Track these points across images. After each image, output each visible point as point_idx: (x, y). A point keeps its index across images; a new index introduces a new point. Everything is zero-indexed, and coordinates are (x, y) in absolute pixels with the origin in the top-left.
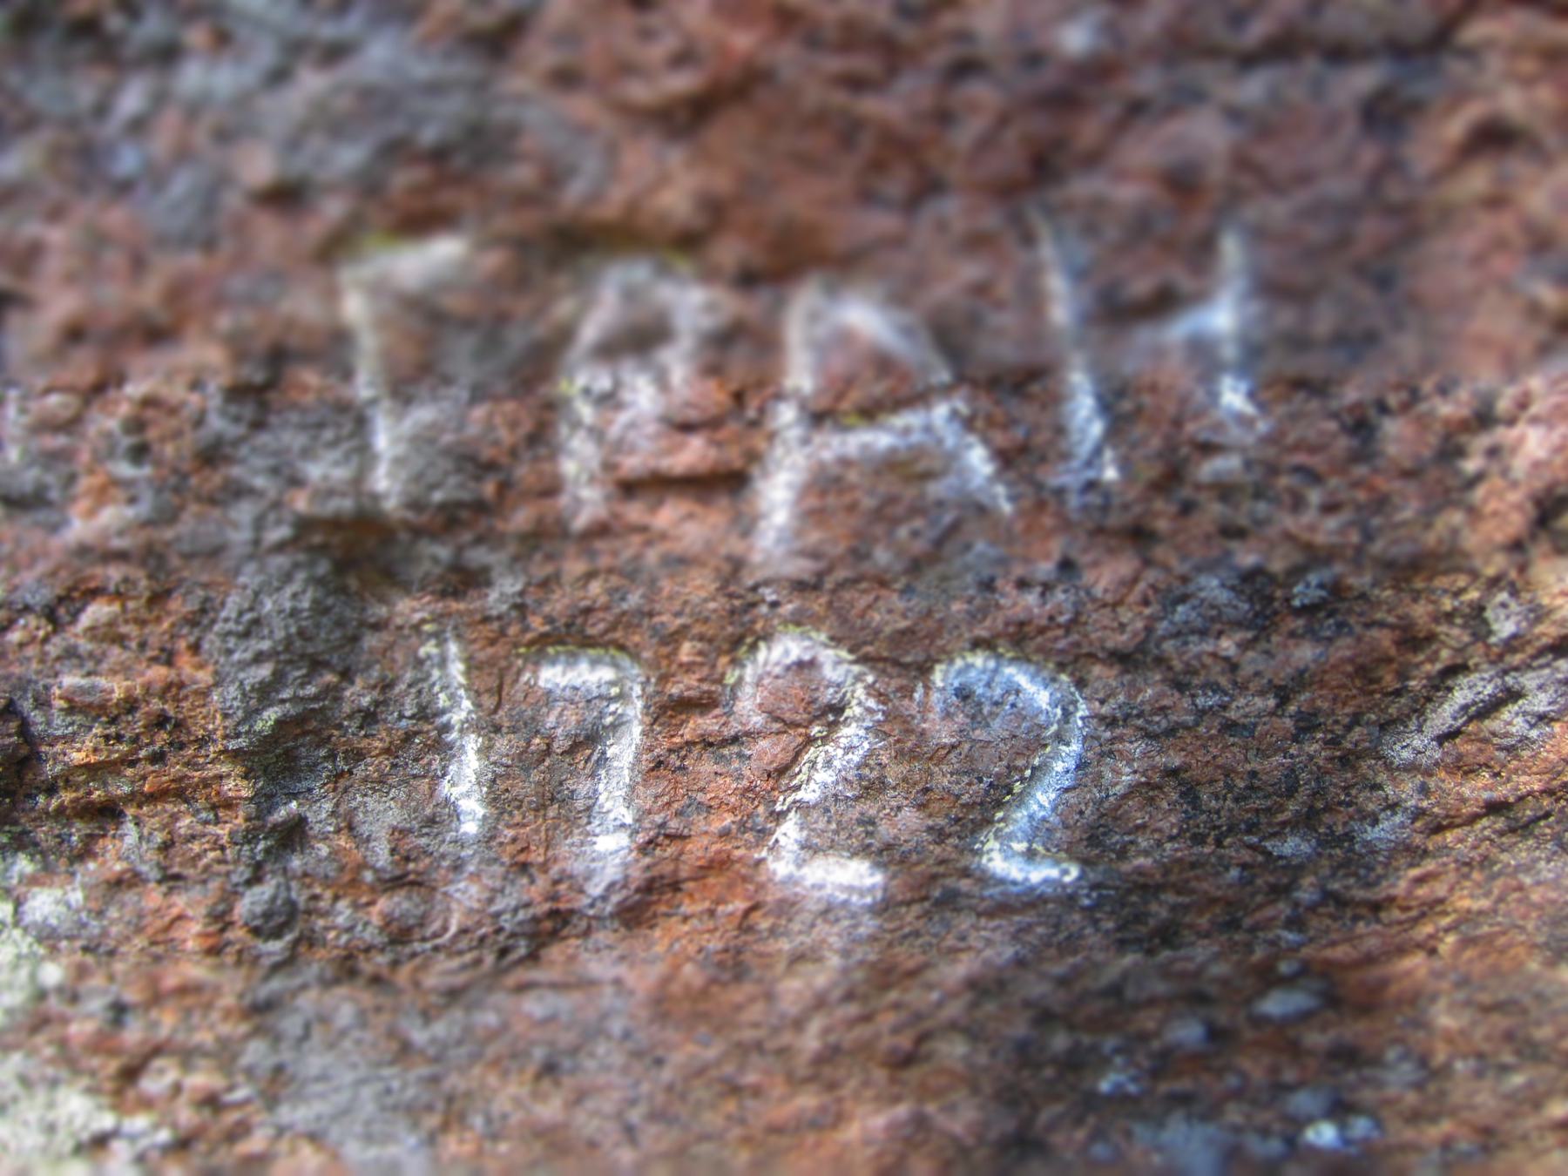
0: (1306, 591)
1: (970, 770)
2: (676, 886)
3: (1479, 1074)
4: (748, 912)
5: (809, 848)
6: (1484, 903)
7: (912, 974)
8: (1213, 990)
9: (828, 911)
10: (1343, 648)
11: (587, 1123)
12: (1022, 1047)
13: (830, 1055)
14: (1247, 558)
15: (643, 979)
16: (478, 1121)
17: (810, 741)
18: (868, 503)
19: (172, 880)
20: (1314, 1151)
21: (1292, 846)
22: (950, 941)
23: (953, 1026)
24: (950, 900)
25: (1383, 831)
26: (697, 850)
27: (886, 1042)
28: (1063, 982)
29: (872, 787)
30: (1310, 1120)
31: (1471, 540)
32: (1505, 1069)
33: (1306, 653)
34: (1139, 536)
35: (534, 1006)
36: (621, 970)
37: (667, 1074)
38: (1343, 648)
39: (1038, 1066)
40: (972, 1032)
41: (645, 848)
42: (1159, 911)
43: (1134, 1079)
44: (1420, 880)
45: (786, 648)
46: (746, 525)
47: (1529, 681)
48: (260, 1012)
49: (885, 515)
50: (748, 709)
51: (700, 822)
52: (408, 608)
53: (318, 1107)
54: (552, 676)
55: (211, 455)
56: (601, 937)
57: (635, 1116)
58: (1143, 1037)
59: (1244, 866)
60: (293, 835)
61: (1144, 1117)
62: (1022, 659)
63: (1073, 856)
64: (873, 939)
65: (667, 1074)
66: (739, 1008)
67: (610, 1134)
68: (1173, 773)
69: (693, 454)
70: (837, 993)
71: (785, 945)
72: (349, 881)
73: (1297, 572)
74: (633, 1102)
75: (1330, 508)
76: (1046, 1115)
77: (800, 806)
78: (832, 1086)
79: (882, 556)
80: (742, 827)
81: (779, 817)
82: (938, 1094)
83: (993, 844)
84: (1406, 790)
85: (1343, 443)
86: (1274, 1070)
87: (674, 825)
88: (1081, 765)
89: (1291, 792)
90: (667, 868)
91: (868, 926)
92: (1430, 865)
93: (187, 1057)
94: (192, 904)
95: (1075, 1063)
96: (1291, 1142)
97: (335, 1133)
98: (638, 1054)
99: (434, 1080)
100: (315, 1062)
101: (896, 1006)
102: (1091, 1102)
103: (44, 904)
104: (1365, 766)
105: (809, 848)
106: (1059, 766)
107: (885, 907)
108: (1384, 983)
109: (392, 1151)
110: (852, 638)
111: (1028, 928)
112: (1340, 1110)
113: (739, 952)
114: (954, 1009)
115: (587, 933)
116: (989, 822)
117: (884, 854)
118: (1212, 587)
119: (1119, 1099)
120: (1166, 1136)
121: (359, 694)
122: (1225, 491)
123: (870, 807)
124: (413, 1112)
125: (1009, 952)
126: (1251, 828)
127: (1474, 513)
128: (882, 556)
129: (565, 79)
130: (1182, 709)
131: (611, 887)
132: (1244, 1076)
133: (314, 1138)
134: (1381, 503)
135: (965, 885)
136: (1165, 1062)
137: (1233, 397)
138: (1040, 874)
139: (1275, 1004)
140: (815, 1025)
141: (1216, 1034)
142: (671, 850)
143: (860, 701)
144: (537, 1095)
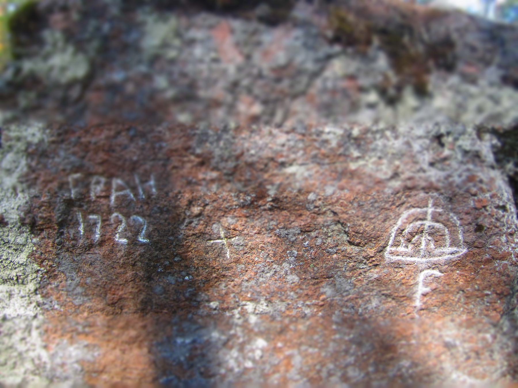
0: (165, 209)
1: (135, 228)
2: (105, 241)
3: (203, 270)
4: (113, 245)
5: (120, 238)
6: (196, 246)
7: (133, 253)
8: (168, 257)
9: (122, 245)
10: (170, 216)
11: (95, 271)
12: (147, 264)
13: (124, 264)
14: (158, 206)
15: (102, 253)
16: (82, 271)
17: (118, 225)
18: (121, 199)
19: (49, 238)
20: (186, 280)
21: (171, 238)
22: (137, 249)
23: (138, 260)
24: (136, 244)
25: (181, 237)
26: (107, 237)
27: (131, 262)
28: (150, 255)
29: (126, 230)
30: (185, 276)
31: (181, 205)
32: (206, 269)
33: (167, 216)
34: (147, 203)
35: (89, 256)
36: (99, 252)
37: (105, 265)
38: (170, 216)
39: (150, 267)
40: (142, 262)
41: (101, 236)
42: (159, 245)
43: (162, 269)
44: (187, 243)
45: (115, 215)
46: (110, 201)
47: (194, 220)
48: (58, 254)
49: (123, 200)
50: (112, 221)
51: (107, 234)
52: (75, 209)
53: (64, 268)
54: (91, 217)
55: (56, 193)
56: (97, 248)
57: (101, 271)
58: (162, 264)
59: (167, 240)
60: (62, 233)
61: (166, 275)
62: (139, 216)
63: (148, 239)
64: (127, 248)
65: (105, 265)
66: (113, 257)
67: (98, 273)
68: (156, 229)
69: (103, 194)
70: (124, 255)
71: (118, 249)
72: (68, 239)
73: (164, 207)
74: (101, 269)
75: (165, 201)
76: (153, 274)
77: (119, 232)
78: (125, 268)
79: (123, 205)
80: (112, 234)
81: (116, 234)
82: (139, 270)
83: (139, 237)
84: (183, 232)
85: (165, 195)
86: (179, 269)
87: (104, 234)
88: (147, 228)
89: (169, 231)
90: (104, 239)
91: (127, 246)
92: (187, 241)
93: (49, 260)
94: (51, 241)
95: (155, 267)
96: (183, 279)
97: (66, 271)
98: (101, 263)
99: (77, 265)
100: (64, 262)
101: (131, 258)
102: (158, 273)
103: (35, 240)
104: (177, 229)
105: (120, 238)
106: (145, 228)
107: (128, 244)
108: (186, 256)
109: (72, 274)
110: (121, 213)
111: (145, 248)
112: (188, 275)
113: (112, 249)
114: (138, 258)
115: (95, 247)
116: (138, 234)
117: (128, 238)
118: (155, 209)
119: (161, 272)
120: (168, 278)
121: (70, 218)
122: (155, 199)
123: (125, 233)
124: (75, 269)
125: (143, 251)
126: (166, 236)
127: (181, 202)
128: (123, 205)
129: (90, 160)
130: (155, 222)
131: (97, 241)
132: (176, 269)
133: (63, 272)
134: (170, 201)
135: (137, 242)
136: (165, 268)
137: (154, 190)
138: (145, 241)
139: (176, 259)
140: (122, 260)
141: (171, 263)
142: (104, 237)
143: (124, 220)
144: (89, 267)
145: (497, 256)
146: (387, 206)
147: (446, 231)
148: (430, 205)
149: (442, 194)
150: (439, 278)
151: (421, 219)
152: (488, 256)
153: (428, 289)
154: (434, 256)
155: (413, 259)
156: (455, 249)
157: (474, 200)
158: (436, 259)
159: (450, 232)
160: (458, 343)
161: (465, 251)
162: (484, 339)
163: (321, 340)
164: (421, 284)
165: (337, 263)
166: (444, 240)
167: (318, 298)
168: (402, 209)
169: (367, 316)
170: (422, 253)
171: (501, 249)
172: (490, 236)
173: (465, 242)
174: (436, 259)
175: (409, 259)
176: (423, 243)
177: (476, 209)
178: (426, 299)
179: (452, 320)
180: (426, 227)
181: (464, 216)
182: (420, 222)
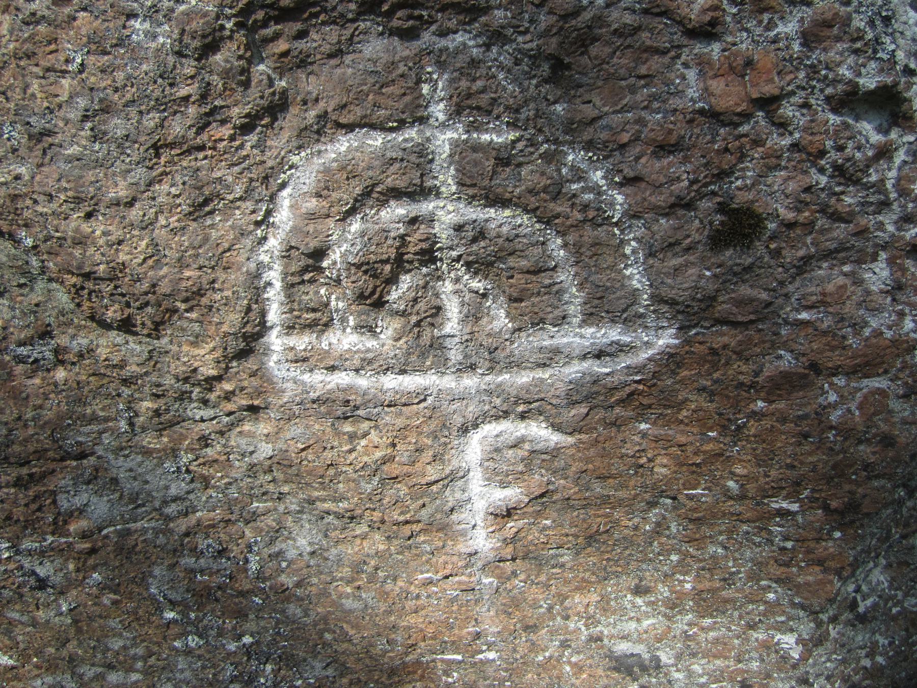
145: (836, 358)
146: (177, 128)
147: (556, 248)
148: (439, 111)
149: (496, 37)
150: (555, 452)
151: (396, 194)
152: (786, 361)
153: (512, 494)
154: (514, 364)
155: (411, 382)
156: (614, 334)
157: (703, 63)
158: (524, 378)
159: (576, 251)
160: (665, 657)
161: (666, 339)
162: (768, 646)
163: (140, 651)
164: (476, 482)
165: (81, 401)
166: (556, 292)
167: (58, 528)
168: (279, 142)
169: (287, 580)
170: (455, 355)
171: (858, 326)
172: (804, 266)
173: (657, 299)
174: (524, 378)
175: (391, 382)
176: (453, 310)
177: (714, 116)
178: (512, 526)
179: (638, 591)
180: (442, 232)
181: (650, 166)
182: (398, 210)
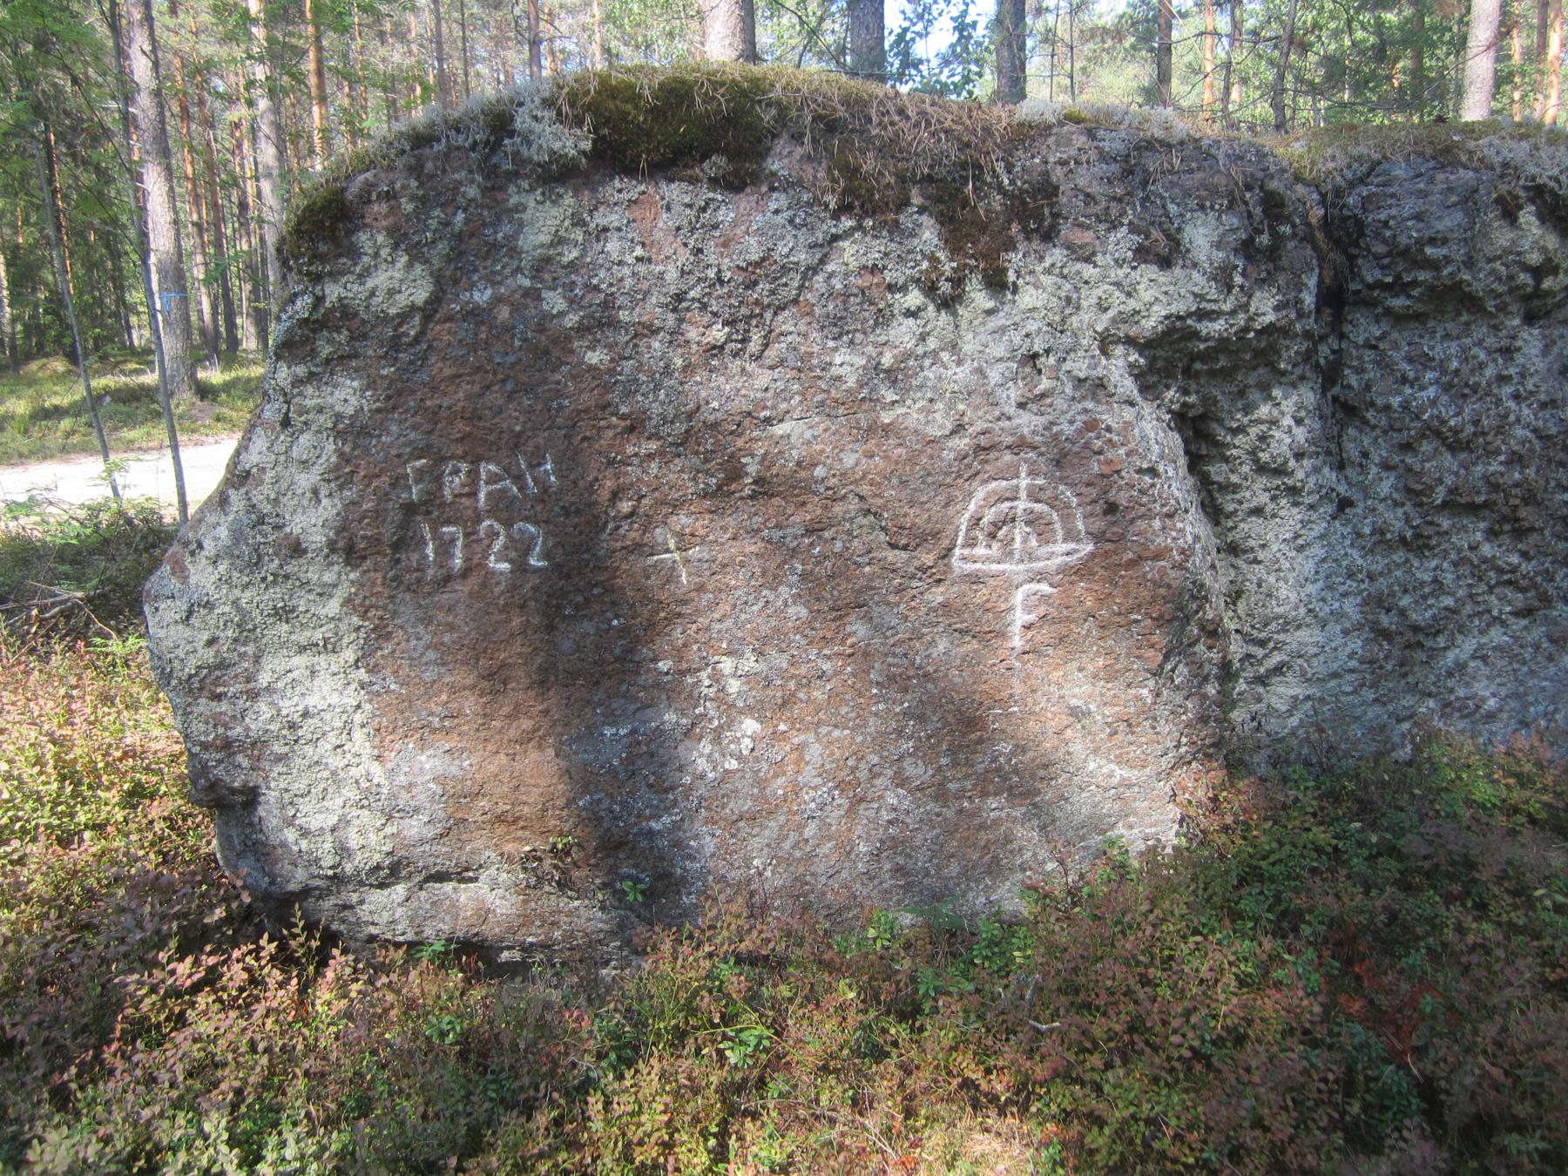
5: (497, 561)
11: (457, 622)
15: (466, 589)
19: (376, 571)
21: (586, 556)
25: (602, 553)
26: (475, 561)
34: (543, 501)
40: (536, 600)
42: (565, 570)
45: (487, 523)
48: (392, 597)
50: (482, 535)
52: (419, 518)
54: (445, 529)
55: (386, 494)
60: (398, 561)
69: (466, 490)
72: (409, 570)
93: (377, 608)
94: (379, 575)
95: (559, 607)
100: (402, 609)
102: (565, 618)
103: (352, 576)
105: (497, 561)
107: (512, 572)
112: (617, 616)
117: (510, 561)
119: (570, 616)
121: (410, 534)
124: (421, 620)
136: (577, 607)
137: (553, 478)
139: (595, 591)
141: (586, 599)
143: (502, 531)
145: (1147, 554)
146: (948, 480)
147: (1055, 516)
148: (1023, 475)
149: (1042, 454)
150: (1049, 596)
151: (1008, 499)
152: (1130, 555)
153: (1032, 617)
154: (1038, 559)
155: (1001, 567)
156: (1071, 546)
157: (1099, 461)
158: (1041, 564)
159: (1062, 517)
160: (1093, 707)
161: (1090, 547)
162: (1138, 698)
163: (853, 715)
164: (1019, 609)
165: (871, 580)
166: (1053, 531)
167: (843, 641)
168: (975, 484)
169: (930, 669)
170: (1017, 556)
171: (1153, 542)
172: (1132, 521)
173: (1087, 533)
174: (1041, 564)
175: (994, 567)
176: (1018, 539)
177: (1103, 476)
178: (1030, 634)
179: (1080, 670)
180: (1019, 512)
181: (1083, 490)
182: (1007, 504)
